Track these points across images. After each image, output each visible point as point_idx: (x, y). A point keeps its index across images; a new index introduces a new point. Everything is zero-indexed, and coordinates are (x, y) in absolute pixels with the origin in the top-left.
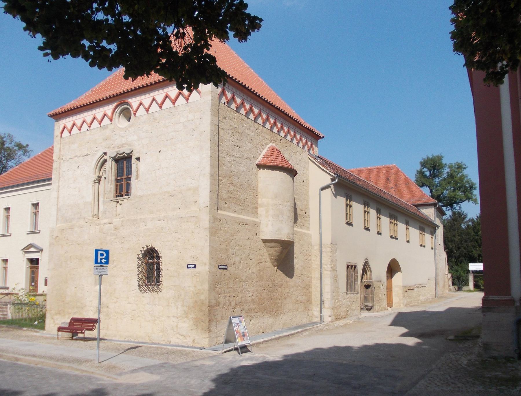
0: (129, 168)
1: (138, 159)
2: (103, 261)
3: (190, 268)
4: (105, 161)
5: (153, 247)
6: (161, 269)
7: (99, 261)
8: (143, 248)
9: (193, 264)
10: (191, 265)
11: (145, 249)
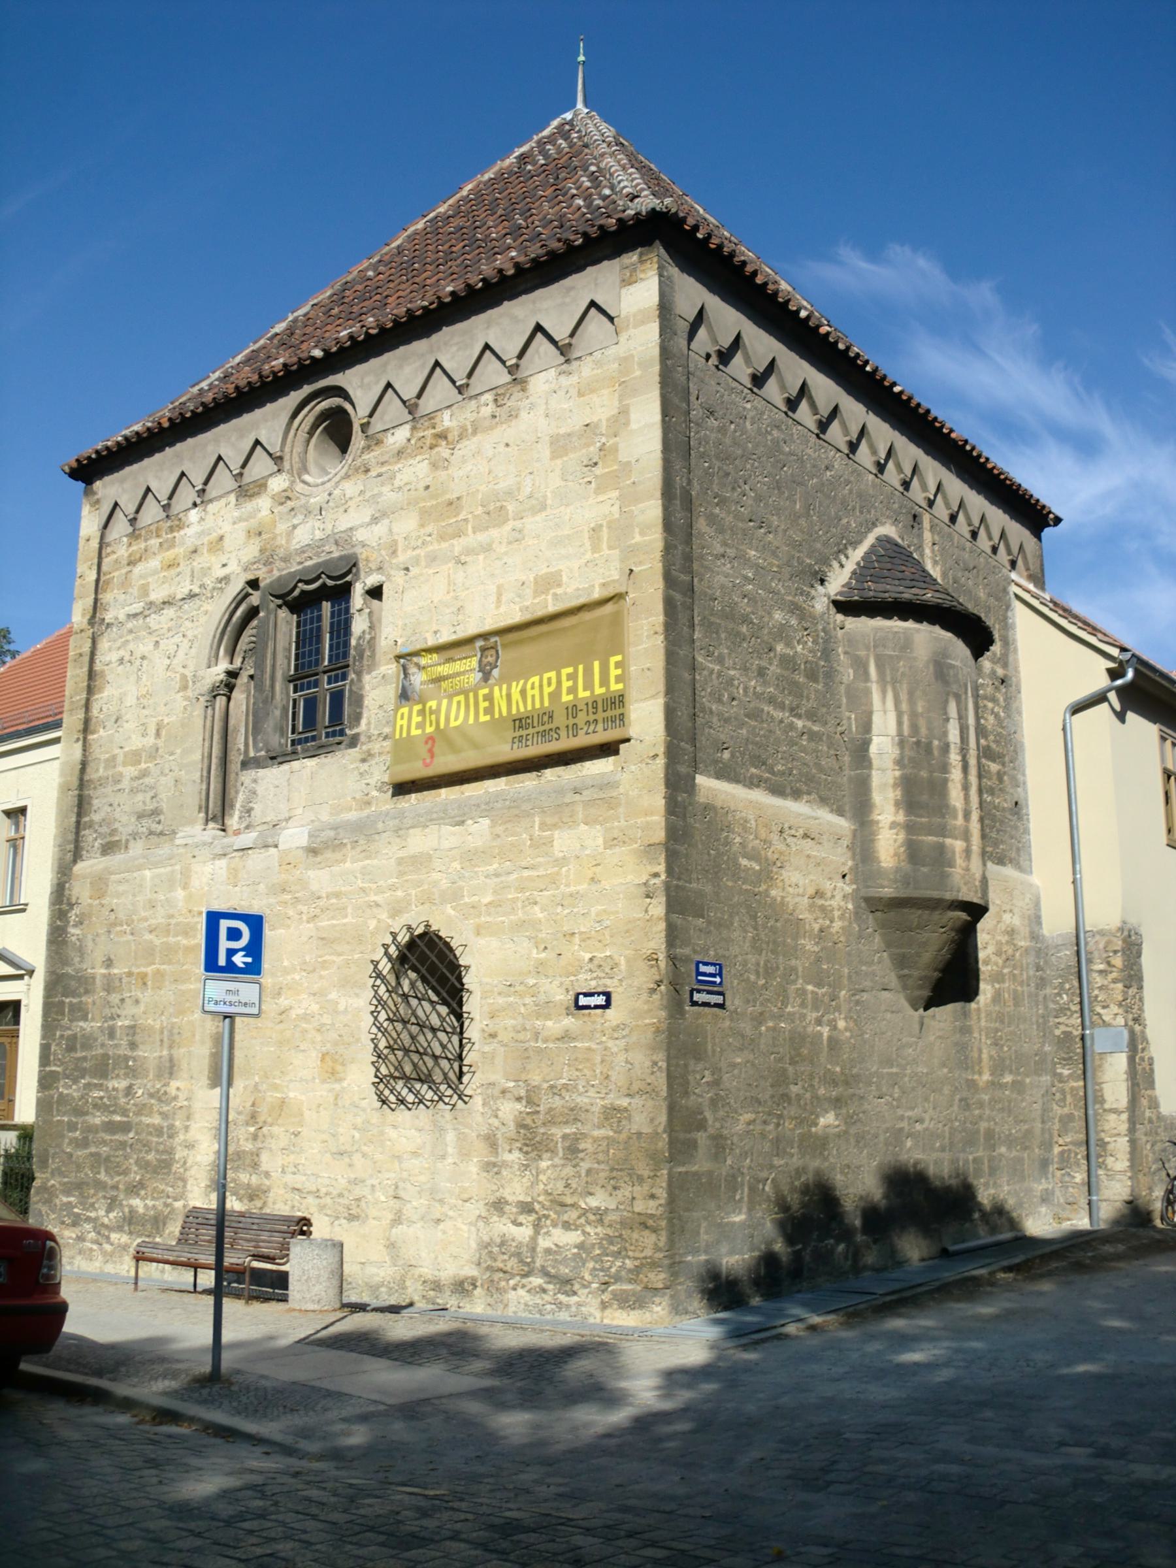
0: (342, 627)
1: (376, 593)
2: (239, 960)
3: (587, 1007)
4: (253, 612)
5: (434, 928)
6: (465, 1015)
7: (222, 961)
8: (394, 935)
9: (600, 990)
10: (591, 995)
11: (403, 938)
